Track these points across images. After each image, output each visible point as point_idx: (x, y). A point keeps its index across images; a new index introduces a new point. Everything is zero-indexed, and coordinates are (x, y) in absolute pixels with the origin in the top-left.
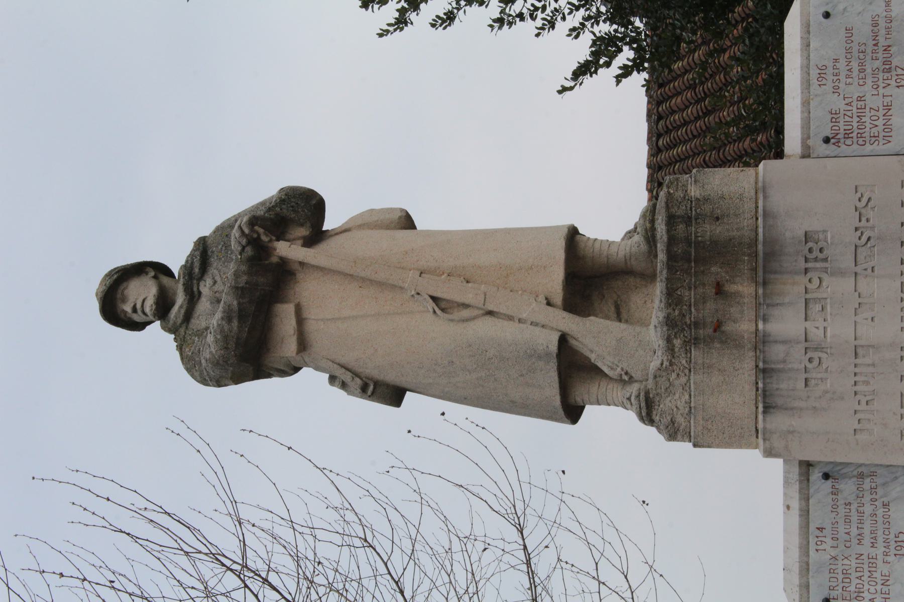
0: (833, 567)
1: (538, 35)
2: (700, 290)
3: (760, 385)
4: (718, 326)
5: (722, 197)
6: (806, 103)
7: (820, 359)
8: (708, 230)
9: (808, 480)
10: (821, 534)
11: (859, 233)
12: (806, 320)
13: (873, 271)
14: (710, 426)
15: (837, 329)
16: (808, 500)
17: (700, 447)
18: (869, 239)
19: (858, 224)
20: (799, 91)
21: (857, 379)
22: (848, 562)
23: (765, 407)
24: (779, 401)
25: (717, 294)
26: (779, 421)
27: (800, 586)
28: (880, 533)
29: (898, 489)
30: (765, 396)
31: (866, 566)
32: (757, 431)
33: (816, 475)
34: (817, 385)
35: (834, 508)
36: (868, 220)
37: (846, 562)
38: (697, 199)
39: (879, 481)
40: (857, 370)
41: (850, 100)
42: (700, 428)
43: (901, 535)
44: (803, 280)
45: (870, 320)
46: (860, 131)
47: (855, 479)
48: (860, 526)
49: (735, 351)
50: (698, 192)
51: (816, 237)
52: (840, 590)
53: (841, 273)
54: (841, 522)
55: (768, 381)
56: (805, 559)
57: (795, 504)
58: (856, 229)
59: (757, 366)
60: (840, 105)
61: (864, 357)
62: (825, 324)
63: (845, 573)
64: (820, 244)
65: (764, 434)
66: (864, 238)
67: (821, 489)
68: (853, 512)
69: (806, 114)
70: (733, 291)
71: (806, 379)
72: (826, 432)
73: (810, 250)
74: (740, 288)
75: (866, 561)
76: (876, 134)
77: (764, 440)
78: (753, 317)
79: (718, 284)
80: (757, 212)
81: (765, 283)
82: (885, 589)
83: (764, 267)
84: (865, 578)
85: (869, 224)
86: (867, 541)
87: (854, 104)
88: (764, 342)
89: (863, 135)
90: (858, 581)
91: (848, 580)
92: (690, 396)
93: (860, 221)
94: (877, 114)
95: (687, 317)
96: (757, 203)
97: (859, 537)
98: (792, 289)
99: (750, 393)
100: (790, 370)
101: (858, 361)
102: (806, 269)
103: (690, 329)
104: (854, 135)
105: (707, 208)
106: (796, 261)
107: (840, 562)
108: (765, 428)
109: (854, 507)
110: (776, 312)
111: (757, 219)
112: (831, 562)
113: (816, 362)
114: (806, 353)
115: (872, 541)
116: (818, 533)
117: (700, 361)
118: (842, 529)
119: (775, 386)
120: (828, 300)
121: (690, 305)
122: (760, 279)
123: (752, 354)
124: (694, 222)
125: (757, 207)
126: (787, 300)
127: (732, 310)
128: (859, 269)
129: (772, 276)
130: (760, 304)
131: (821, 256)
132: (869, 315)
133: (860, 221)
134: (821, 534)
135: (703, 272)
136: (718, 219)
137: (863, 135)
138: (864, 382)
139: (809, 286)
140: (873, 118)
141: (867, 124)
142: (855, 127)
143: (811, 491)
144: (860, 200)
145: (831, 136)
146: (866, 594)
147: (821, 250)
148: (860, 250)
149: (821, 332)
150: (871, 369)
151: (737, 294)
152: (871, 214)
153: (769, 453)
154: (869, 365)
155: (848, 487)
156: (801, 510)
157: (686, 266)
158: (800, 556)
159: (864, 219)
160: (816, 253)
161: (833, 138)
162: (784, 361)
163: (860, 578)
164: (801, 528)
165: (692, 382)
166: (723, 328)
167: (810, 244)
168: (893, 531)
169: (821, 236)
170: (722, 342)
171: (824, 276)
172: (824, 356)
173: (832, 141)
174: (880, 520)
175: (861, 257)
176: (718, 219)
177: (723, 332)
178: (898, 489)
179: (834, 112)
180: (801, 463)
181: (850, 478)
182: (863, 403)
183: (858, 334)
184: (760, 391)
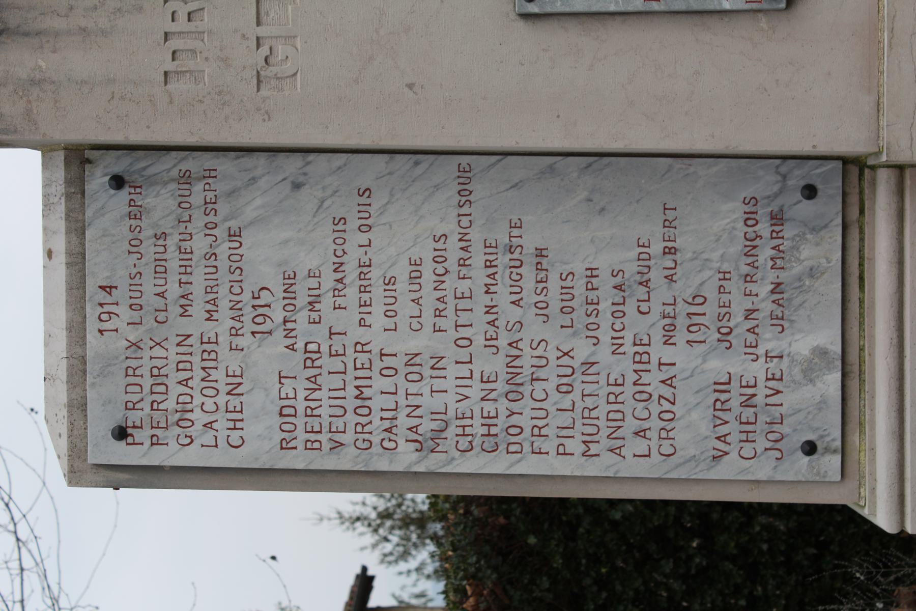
0: (133, 363)
9: (83, 193)
10: (109, 299)
16: (84, 233)
22: (163, 353)
27: (70, 405)
28: (223, 290)
29: (258, 202)
31: (196, 359)
35: (135, 246)
37: (158, 352)
39: (221, 187)
43: (264, 293)
47: (174, 186)
48: (184, 278)
52: (147, 409)
54: (148, 272)
56: (79, 351)
57: (60, 245)
63: (157, 375)
67: (107, 208)
75: (197, 348)
82: (234, 402)
84: (195, 383)
86: (198, 309)
90: (182, 389)
91: (162, 389)
97: (183, 302)
107: (146, 354)
112: (129, 353)
115: (209, 307)
116: (102, 296)
118: (149, 286)
134: (109, 299)
143: (89, 213)
146: (197, 415)
155: (160, 203)
156: (69, 253)
158: (69, 346)
163: (184, 382)
164: (70, 288)
168: (249, 287)
174: (223, 263)
178: (258, 202)
181: (165, 184)
182: (182, 16)
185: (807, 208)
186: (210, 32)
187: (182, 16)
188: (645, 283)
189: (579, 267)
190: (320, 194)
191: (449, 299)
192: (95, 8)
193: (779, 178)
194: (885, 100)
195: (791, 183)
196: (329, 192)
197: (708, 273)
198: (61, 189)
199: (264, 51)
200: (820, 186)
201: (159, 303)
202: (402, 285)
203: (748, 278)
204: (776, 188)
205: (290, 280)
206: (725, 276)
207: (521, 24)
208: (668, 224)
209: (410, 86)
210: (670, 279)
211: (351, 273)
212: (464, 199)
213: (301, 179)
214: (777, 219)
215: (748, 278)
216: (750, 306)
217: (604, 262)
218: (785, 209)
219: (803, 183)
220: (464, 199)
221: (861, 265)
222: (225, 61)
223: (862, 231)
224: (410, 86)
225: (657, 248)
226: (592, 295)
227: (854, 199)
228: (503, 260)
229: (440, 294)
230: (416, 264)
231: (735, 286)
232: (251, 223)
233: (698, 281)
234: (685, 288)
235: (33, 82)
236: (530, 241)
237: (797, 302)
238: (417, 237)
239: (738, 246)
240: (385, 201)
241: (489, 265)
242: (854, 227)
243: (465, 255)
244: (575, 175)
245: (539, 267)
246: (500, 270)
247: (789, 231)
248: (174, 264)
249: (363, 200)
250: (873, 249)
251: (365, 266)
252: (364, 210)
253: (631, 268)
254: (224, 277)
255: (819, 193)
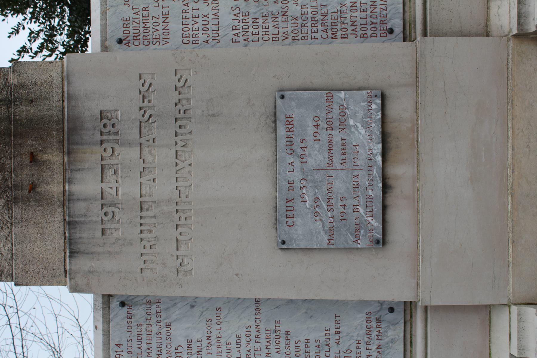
1: (9, 37)
2: (19, 159)
3: (67, 235)
4: (33, 188)
5: (36, 84)
6: (104, 13)
7: (113, 212)
8: (24, 110)
9: (109, 307)
10: (119, 350)
11: (142, 112)
12: (102, 182)
13: (153, 142)
14: (28, 269)
15: (127, 189)
16: (109, 323)
17: (20, 285)
18: (150, 116)
19: (142, 105)
20: (99, 4)
21: (142, 228)
23: (70, 252)
24: (82, 247)
25: (31, 162)
26: (82, 264)
28: (164, 346)
29: (177, 312)
30: (70, 244)
32: (65, 271)
33: (115, 304)
34: (111, 233)
35: (129, 329)
36: (149, 101)
38: (15, 86)
39: (163, 307)
40: (142, 221)
41: (138, 10)
42: (20, 270)
44: (99, 149)
45: (152, 180)
46: (146, 34)
47: (144, 306)
48: (149, 342)
49: (47, 208)
50: (16, 80)
51: (110, 115)
53: (130, 144)
54: (134, 339)
55: (72, 231)
57: (100, 326)
58: (141, 109)
59: (65, 220)
60: (129, 13)
61: (148, 210)
62: (117, 185)
64: (112, 121)
65: (70, 274)
66: (147, 116)
67: (119, 314)
68: (144, 332)
69: (104, 22)
70: (45, 159)
71: (102, 229)
72: (121, 270)
73: (105, 126)
74: (51, 157)
76: (157, 37)
77: (70, 279)
78: (61, 181)
79: (32, 154)
80: (63, 96)
81: (69, 153)
83: (69, 140)
85: (150, 105)
87: (140, 13)
88: (69, 200)
89: (148, 37)
92: (12, 244)
93: (143, 102)
94: (158, 21)
95: (9, 181)
96: (63, 88)
97: (148, 351)
98: (91, 157)
99: (59, 241)
100: (90, 222)
101: (143, 214)
102: (101, 141)
103: (11, 190)
104: (141, 37)
105: (23, 93)
106: (94, 134)
108: (70, 269)
109: (144, 328)
110: (78, 175)
111: (63, 101)
113: (110, 215)
114: (102, 208)
115: (158, 353)
116: (117, 348)
117: (19, 217)
118: (135, 345)
119: (78, 235)
120: (119, 166)
121: (11, 171)
122: (66, 150)
123: (60, 210)
124: (13, 103)
125: (63, 92)
126: (87, 166)
127: (45, 175)
128: (143, 140)
129: (75, 147)
130: (66, 170)
131: (113, 130)
132: (151, 177)
133: (143, 102)
134: (119, 350)
135: (21, 144)
136: (32, 101)
137: (148, 37)
138: (148, 230)
139: (104, 154)
140: (154, 24)
141: (150, 29)
142: (141, 31)
143: (111, 316)
144: (143, 85)
145: (123, 38)
147: (113, 126)
148: (143, 125)
149: (114, 191)
150: (153, 220)
151: (48, 161)
152: (152, 97)
153: (74, 289)
154: (151, 217)
155: (139, 312)
156: (104, 331)
157: (7, 140)
159: (146, 100)
160: (109, 128)
161: (125, 39)
162: (85, 215)
164: (104, 344)
165: (13, 233)
166: (38, 190)
167: (105, 121)
169: (113, 115)
170: (36, 201)
171: (116, 146)
172: (116, 210)
173: (124, 42)
174: (164, 336)
175: (144, 131)
176: (32, 101)
177: (38, 192)
178: (177, 312)
179: (125, 19)
180: (103, 296)
181: (141, 305)
182: (148, 247)
183: (143, 192)
184: (67, 240)
185: (390, 316)
186: (159, 253)
187: (148, 247)
188: (328, 345)
189: (302, 339)
190: (201, 310)
191: (252, 351)
192: (114, 243)
193: (380, 305)
194: (420, 281)
195: (384, 306)
196: (205, 309)
197: (352, 341)
198: (100, 305)
199: (180, 260)
200: (395, 308)
201: (139, 351)
202: (233, 345)
203: (368, 343)
204: (378, 308)
205: (190, 343)
206: (359, 342)
207: (280, 251)
208: (337, 322)
209: (237, 275)
210: (338, 343)
211: (214, 340)
212: (257, 312)
213: (194, 304)
214: (379, 320)
215: (368, 343)
216: (368, 354)
217: (312, 337)
218: (382, 316)
219: (389, 307)
220: (257, 312)
221: (411, 337)
222: (164, 264)
223: (411, 324)
224: (237, 275)
225: (332, 331)
226: (307, 349)
227: (408, 312)
228: (273, 336)
229: (248, 349)
230: (239, 337)
231: (363, 346)
232: (174, 321)
233: (348, 344)
234: (343, 347)
235: (90, 272)
236: (283, 329)
237: (386, 352)
238: (239, 327)
239: (364, 331)
240: (226, 313)
241: (267, 337)
242: (408, 323)
243: (258, 334)
244: (301, 303)
245: (287, 339)
246: (271, 339)
247: (383, 325)
248: (144, 336)
249: (218, 312)
250: (416, 332)
251: (219, 338)
252: (218, 316)
253: (322, 339)
254: (164, 341)
255: (395, 311)
